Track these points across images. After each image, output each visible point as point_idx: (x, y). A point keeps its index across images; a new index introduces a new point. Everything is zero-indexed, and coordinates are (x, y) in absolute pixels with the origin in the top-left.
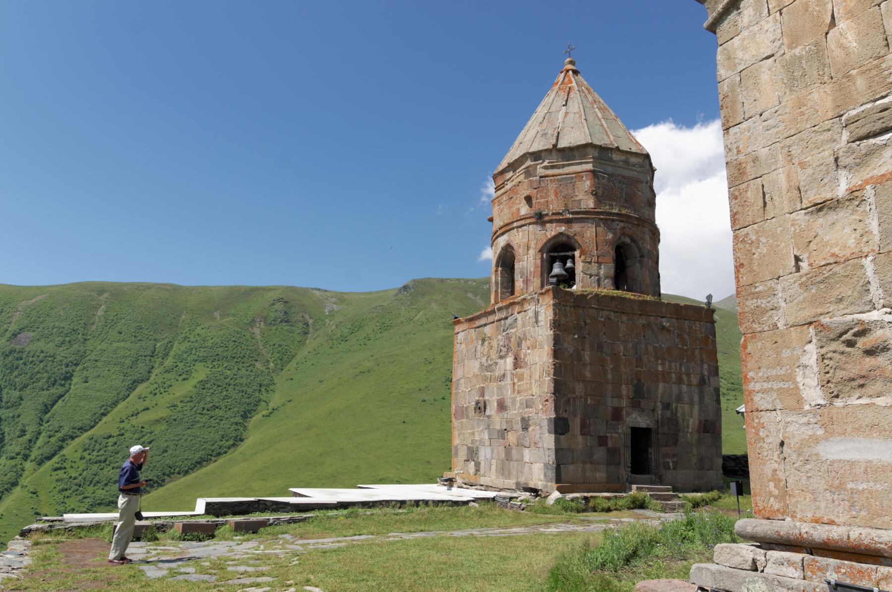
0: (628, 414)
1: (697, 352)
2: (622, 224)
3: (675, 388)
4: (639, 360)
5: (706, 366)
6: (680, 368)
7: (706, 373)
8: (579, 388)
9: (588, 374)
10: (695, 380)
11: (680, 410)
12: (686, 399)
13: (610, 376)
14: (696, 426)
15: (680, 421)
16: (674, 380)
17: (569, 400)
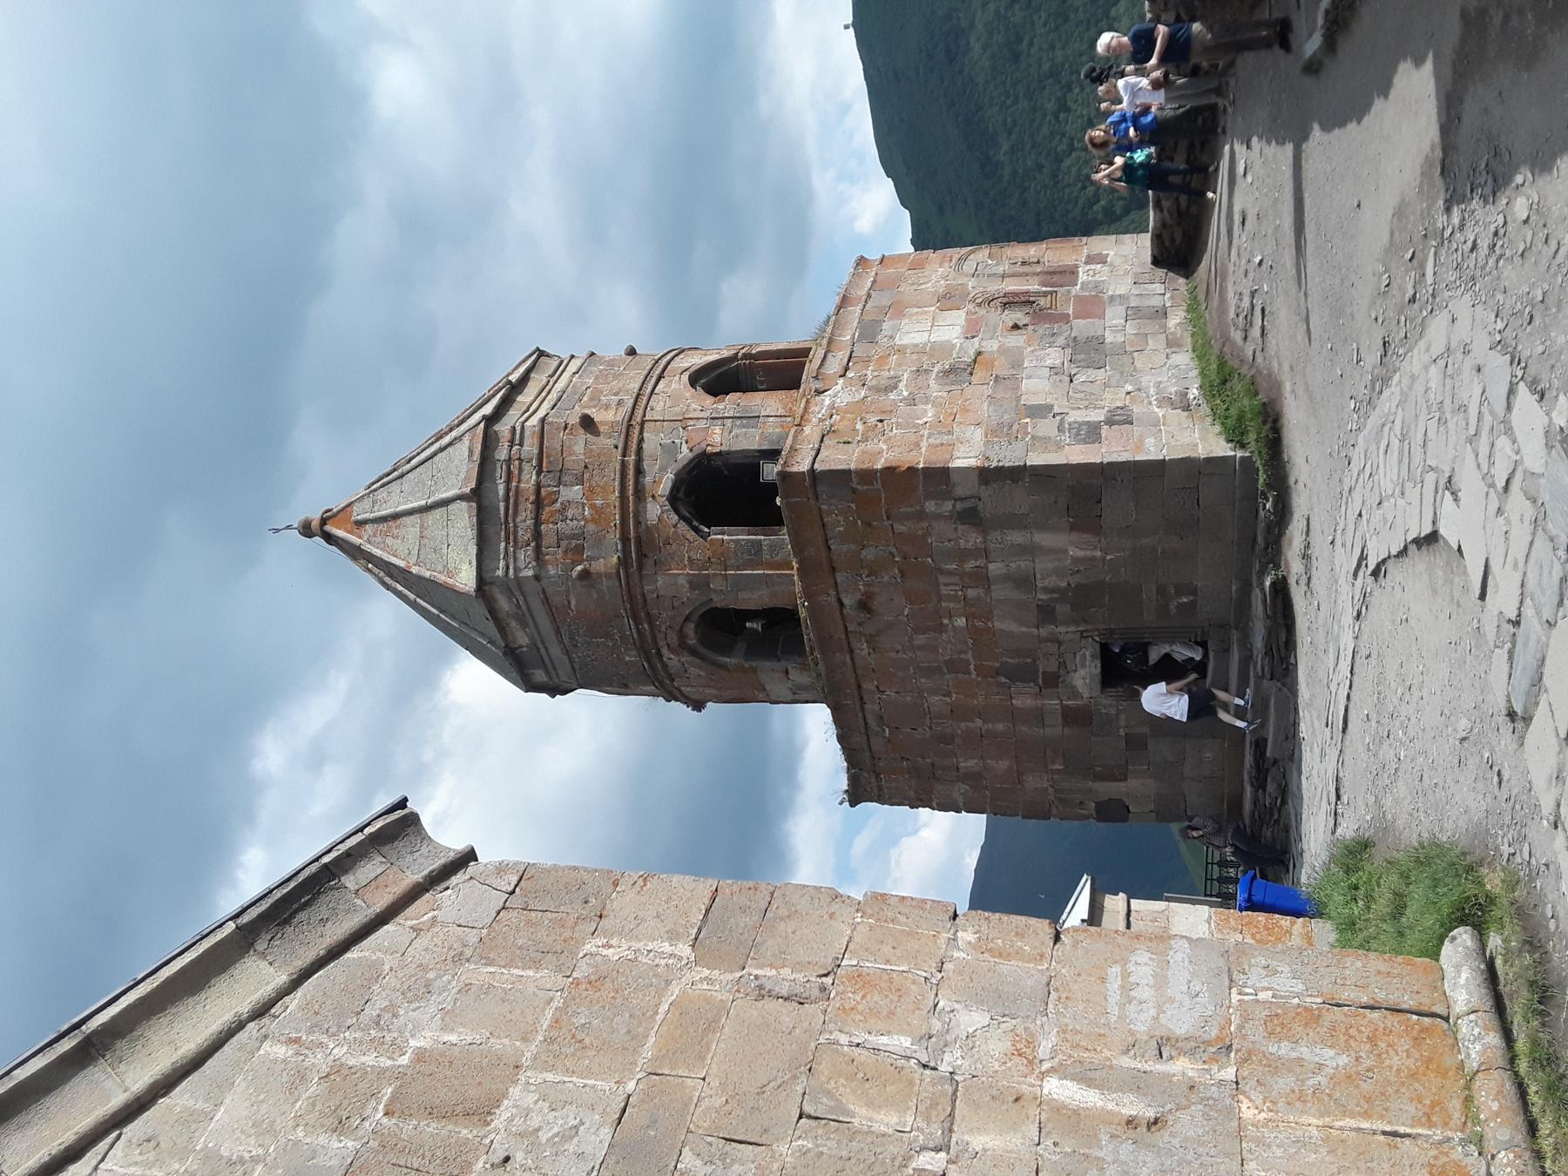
0: (1075, 694)
1: (899, 528)
2: (665, 651)
3: (1000, 592)
4: (955, 666)
5: (930, 506)
6: (950, 573)
7: (948, 506)
8: (1035, 782)
9: (1004, 765)
10: (972, 539)
11: (1051, 582)
12: (1023, 564)
13: (1000, 727)
14: (1086, 537)
15: (1074, 581)
16: (981, 591)
17: (1061, 800)
